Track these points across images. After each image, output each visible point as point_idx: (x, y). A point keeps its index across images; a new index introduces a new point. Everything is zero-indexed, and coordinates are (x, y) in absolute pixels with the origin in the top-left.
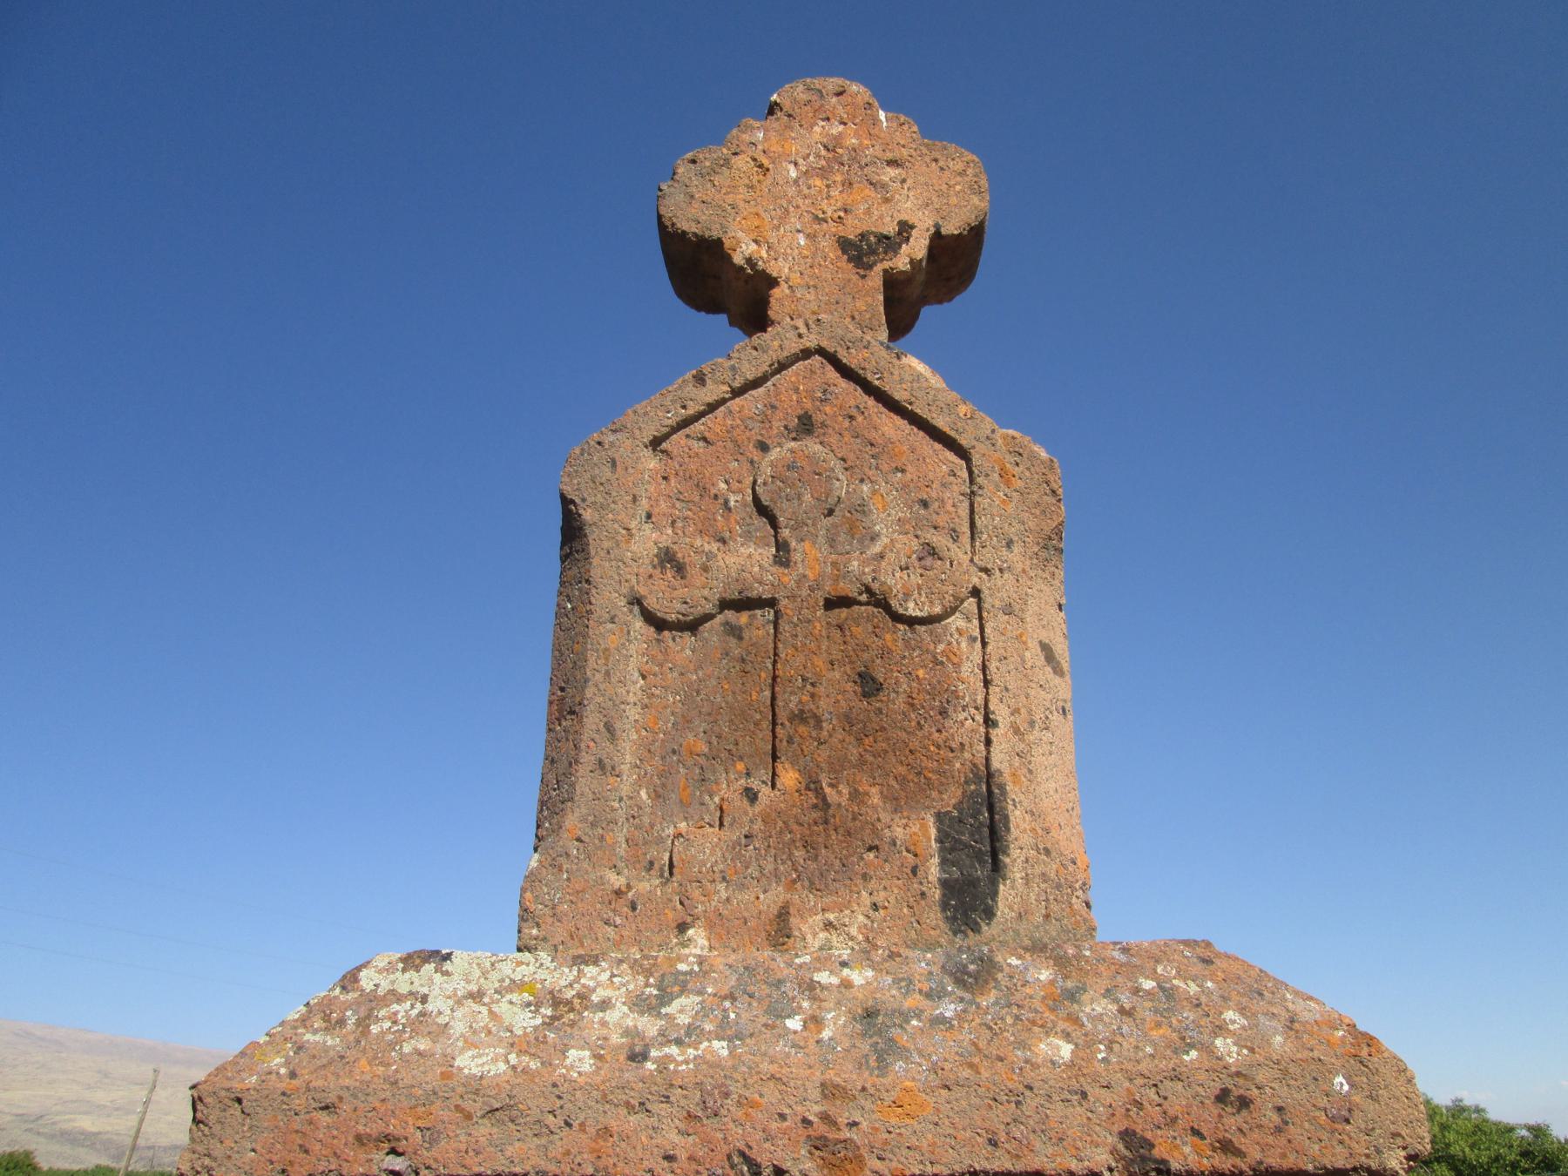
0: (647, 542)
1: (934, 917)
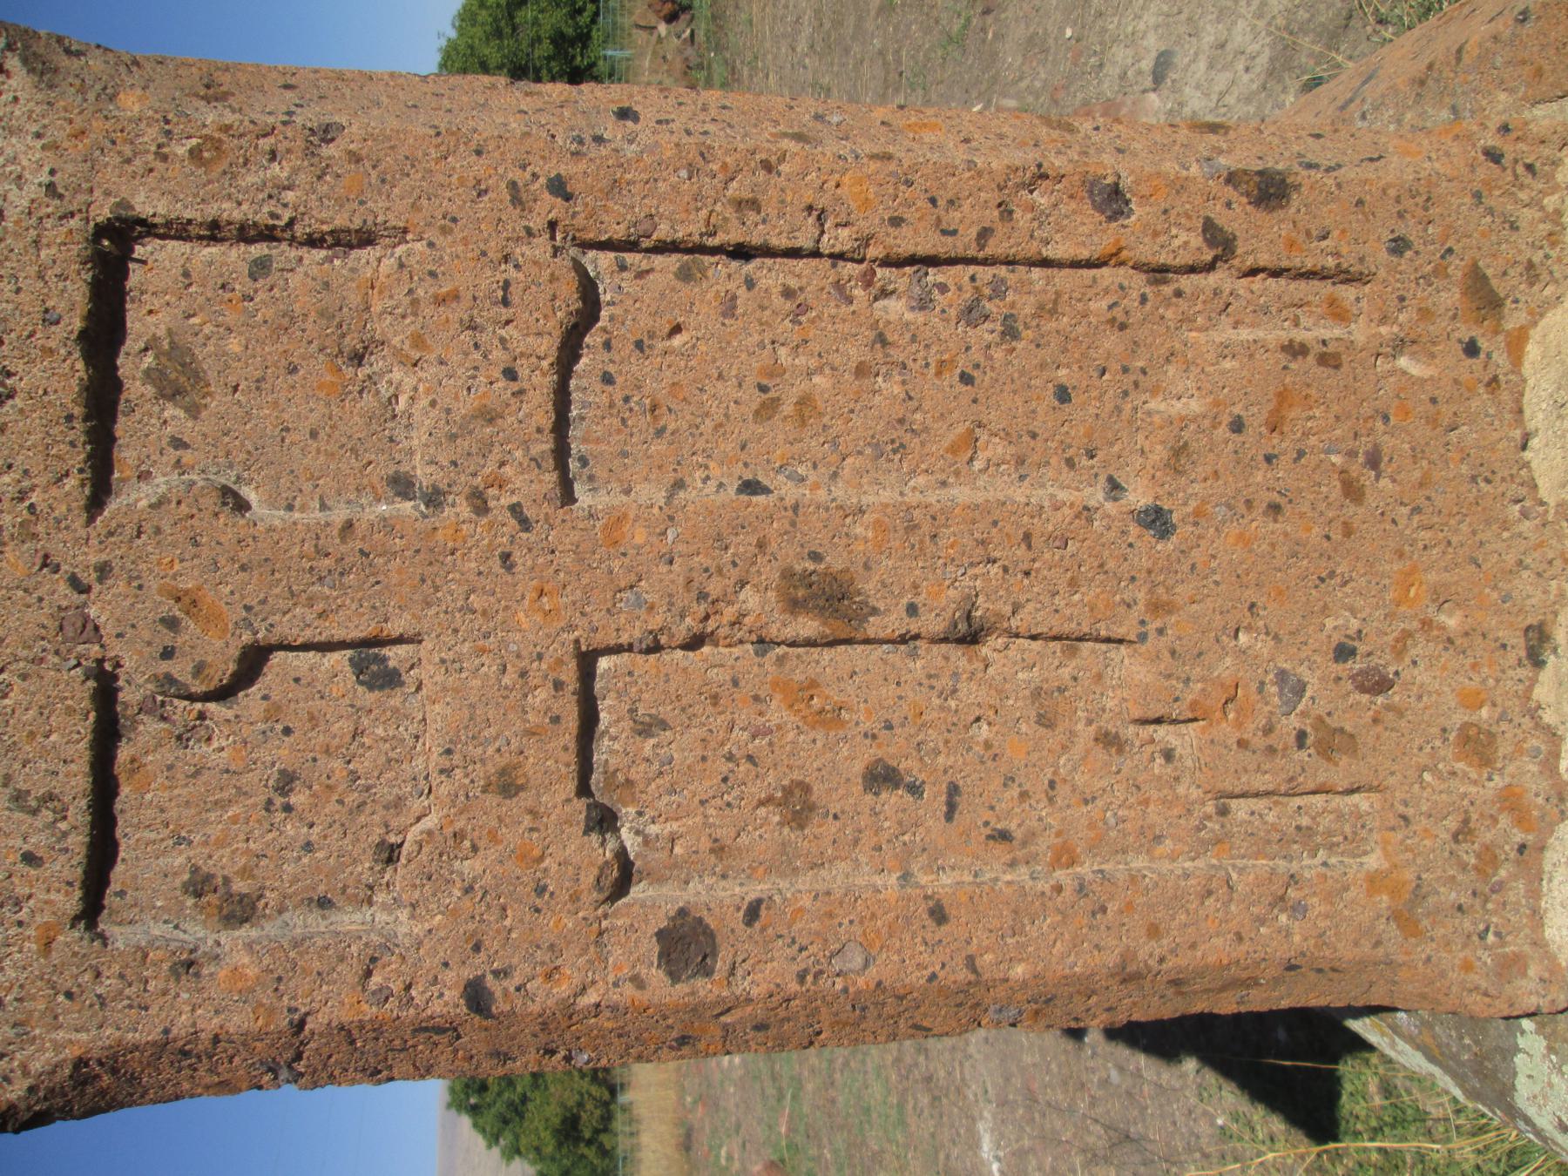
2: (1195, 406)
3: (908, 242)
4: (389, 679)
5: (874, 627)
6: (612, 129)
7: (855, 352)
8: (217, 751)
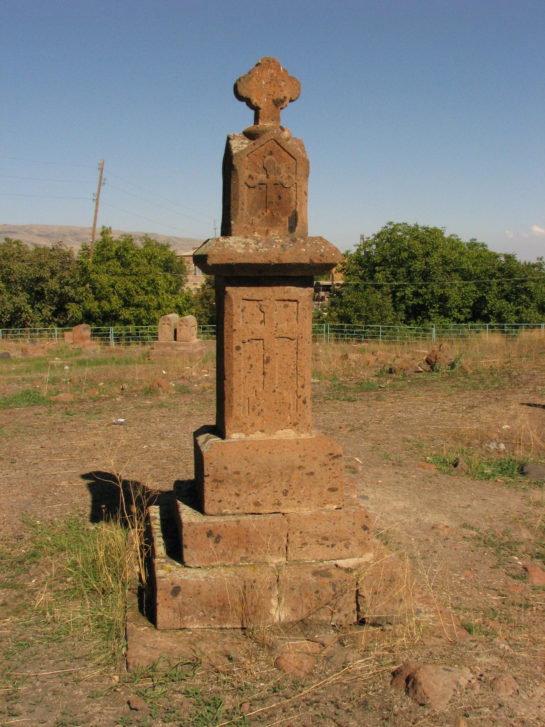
0: (247, 173)
1: (287, 231)
2: (285, 395)
3: (298, 368)
4: (261, 323)
5: (265, 365)
6: (307, 341)
7: (289, 363)
8: (256, 309)
